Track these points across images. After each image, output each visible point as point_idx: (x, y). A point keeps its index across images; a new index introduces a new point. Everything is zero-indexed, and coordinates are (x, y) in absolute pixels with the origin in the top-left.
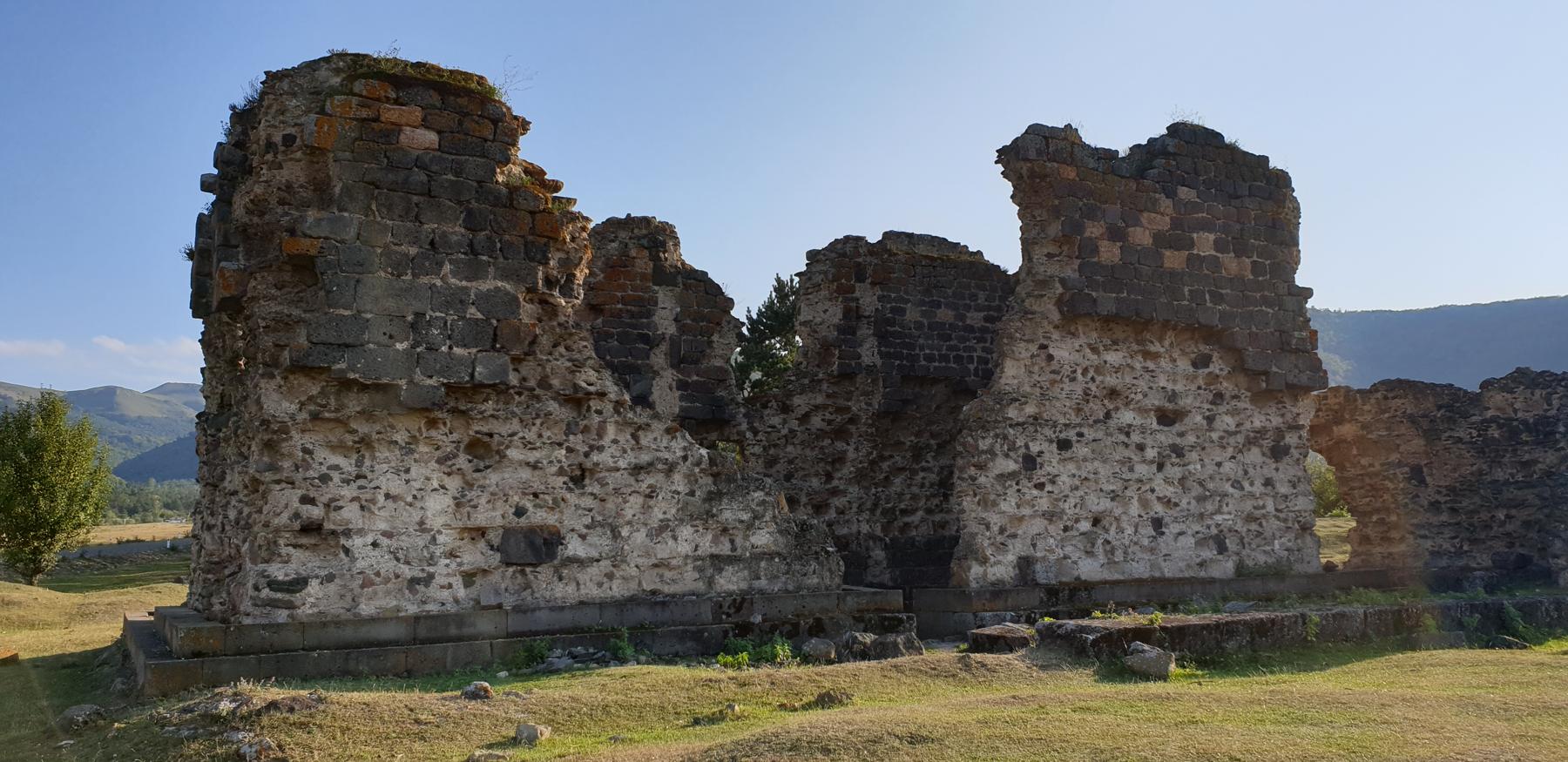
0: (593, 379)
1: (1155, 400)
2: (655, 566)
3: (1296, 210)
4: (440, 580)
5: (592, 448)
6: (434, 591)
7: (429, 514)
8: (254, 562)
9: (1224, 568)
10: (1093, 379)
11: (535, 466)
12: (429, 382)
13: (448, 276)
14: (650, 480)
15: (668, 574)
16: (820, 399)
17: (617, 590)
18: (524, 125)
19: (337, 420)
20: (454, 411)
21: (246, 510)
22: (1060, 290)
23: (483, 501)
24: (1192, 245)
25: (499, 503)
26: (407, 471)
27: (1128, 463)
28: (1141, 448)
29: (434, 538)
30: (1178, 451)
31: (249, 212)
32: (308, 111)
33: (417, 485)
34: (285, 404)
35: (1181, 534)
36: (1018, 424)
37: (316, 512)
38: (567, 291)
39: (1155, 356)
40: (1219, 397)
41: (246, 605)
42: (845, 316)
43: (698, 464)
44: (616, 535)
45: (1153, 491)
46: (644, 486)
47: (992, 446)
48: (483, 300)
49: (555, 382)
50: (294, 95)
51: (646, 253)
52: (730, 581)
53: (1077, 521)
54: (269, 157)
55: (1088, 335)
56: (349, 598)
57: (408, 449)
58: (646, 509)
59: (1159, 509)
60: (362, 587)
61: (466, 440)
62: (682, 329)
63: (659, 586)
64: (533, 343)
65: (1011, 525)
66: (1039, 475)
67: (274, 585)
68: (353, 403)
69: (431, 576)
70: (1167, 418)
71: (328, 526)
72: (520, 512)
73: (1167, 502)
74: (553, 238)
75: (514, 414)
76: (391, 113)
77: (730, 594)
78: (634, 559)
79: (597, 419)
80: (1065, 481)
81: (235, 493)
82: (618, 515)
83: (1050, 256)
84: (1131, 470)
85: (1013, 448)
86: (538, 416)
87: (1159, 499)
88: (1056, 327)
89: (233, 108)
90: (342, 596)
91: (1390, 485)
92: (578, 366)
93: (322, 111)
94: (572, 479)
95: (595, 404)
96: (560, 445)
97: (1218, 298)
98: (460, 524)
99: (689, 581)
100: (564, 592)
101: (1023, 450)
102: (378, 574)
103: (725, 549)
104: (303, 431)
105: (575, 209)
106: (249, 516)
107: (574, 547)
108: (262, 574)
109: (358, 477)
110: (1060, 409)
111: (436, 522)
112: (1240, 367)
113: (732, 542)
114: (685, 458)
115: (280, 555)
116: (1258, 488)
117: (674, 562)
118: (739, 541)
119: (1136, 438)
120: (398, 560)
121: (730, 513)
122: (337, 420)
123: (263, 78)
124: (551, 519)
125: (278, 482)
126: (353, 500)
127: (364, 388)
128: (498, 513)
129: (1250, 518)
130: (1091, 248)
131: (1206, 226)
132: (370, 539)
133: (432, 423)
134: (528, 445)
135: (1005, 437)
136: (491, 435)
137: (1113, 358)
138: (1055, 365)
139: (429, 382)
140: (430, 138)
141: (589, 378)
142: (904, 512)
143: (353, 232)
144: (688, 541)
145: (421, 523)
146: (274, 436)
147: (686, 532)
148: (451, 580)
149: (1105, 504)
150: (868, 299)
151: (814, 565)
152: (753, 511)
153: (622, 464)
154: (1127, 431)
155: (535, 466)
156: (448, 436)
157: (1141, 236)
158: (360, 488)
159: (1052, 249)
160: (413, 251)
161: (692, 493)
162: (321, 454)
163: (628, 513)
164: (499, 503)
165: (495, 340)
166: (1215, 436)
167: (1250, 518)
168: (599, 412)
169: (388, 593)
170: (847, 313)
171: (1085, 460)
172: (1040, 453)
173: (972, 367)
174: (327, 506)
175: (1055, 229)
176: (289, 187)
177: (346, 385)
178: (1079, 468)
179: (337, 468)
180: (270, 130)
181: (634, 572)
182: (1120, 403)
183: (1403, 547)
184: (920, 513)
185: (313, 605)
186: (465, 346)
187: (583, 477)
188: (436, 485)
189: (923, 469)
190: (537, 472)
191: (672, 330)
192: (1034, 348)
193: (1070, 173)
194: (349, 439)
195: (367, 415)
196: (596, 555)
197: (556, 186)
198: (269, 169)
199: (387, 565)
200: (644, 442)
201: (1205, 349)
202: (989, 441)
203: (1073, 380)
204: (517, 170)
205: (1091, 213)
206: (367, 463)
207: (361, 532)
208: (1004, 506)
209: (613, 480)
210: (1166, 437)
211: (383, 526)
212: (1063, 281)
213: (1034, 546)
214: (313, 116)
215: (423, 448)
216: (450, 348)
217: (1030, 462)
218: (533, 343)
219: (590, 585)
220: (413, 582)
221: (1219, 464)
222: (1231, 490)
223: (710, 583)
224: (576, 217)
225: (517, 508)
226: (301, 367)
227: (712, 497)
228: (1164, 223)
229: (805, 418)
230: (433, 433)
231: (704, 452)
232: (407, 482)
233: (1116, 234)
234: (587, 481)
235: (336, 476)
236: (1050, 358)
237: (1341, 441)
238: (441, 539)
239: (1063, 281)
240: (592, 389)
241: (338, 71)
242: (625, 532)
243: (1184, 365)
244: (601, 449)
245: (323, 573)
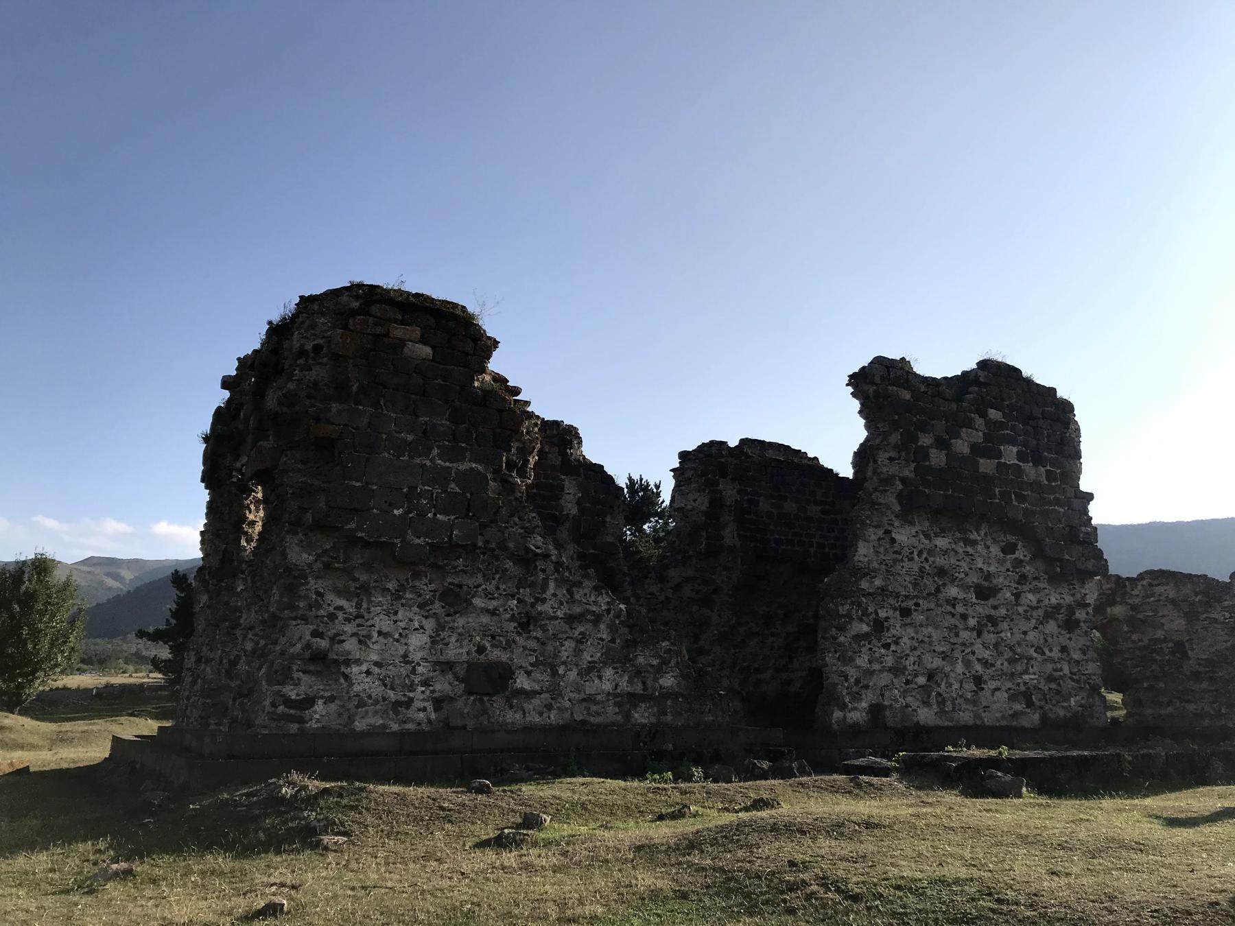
0: (540, 544)
1: (974, 579)
2: (584, 700)
3: (1078, 430)
4: (418, 704)
5: (537, 600)
6: (411, 713)
7: (411, 649)
8: (269, 683)
9: (1033, 719)
10: (926, 560)
11: (493, 613)
12: (418, 541)
13: (435, 458)
14: (581, 629)
15: (594, 708)
16: (690, 572)
17: (554, 718)
18: (495, 344)
19: (344, 570)
20: (434, 566)
21: (262, 643)
22: (900, 487)
23: (453, 639)
24: (999, 455)
25: (465, 642)
26: (396, 613)
27: (954, 629)
28: (964, 617)
29: (414, 669)
30: (993, 621)
31: (280, 403)
32: (334, 327)
33: (402, 624)
34: (305, 556)
35: (998, 689)
36: (869, 594)
37: (324, 644)
38: (523, 475)
39: (973, 543)
40: (1023, 579)
41: (261, 719)
42: (710, 503)
43: (618, 616)
44: (554, 673)
45: (973, 653)
46: (577, 633)
47: (850, 611)
48: (463, 478)
49: (511, 545)
50: (323, 314)
51: (556, 449)
52: (642, 716)
53: (916, 676)
54: (301, 361)
56: (345, 716)
57: (397, 596)
58: (578, 652)
59: (979, 667)
60: (357, 707)
61: (441, 590)
62: (582, 510)
63: (587, 718)
64: (496, 512)
65: (869, 675)
66: (887, 637)
67: (288, 702)
68: (358, 558)
69: (411, 700)
70: (984, 593)
71: (333, 656)
72: (481, 650)
73: (985, 663)
74: (516, 431)
75: (479, 570)
76: (398, 332)
77: (643, 726)
78: (569, 694)
79: (542, 576)
81: (252, 628)
82: (556, 656)
83: (891, 459)
84: (957, 635)
85: (865, 613)
86: (497, 572)
87: (978, 660)
88: (897, 516)
89: (270, 323)
90: (340, 715)
91: (1158, 658)
92: (529, 532)
93: (345, 327)
94: (520, 625)
95: (540, 564)
96: (513, 596)
97: (1021, 498)
98: (434, 659)
99: (611, 713)
100: (513, 717)
102: (370, 697)
103: (638, 688)
104: (317, 578)
105: (529, 409)
106: (266, 645)
107: (522, 682)
108: (278, 693)
109: (357, 617)
110: (902, 583)
111: (417, 656)
112: (1039, 554)
113: (644, 683)
114: (608, 611)
115: (292, 679)
116: (1056, 654)
117: (599, 697)
118: (649, 682)
119: (960, 609)
120: (385, 685)
121: (643, 659)
122: (344, 570)
123: (297, 300)
124: (504, 657)
125: (295, 619)
126: (353, 635)
127: (367, 544)
128: (464, 650)
129: (1050, 679)
130: (923, 453)
131: (1011, 441)
132: (364, 668)
133: (417, 575)
134: (489, 596)
135: (859, 605)
136: (460, 586)
137: (941, 543)
138: (896, 547)
139: (418, 541)
140: (427, 351)
141: (536, 542)
142: (757, 670)
143: (366, 421)
144: (608, 681)
145: (405, 656)
146: (293, 579)
147: (608, 673)
148: (426, 704)
149: (938, 662)
150: (729, 492)
151: (709, 706)
152: (661, 657)
153: (559, 614)
154: (953, 602)
155: (493, 613)
156: (426, 587)
157: (961, 446)
158: (359, 625)
159: (893, 454)
160: (410, 438)
162: (330, 597)
163: (564, 655)
164: (465, 642)
165: (468, 510)
166: (1021, 609)
167: (1050, 679)
168: (543, 571)
169: (376, 713)
170: (713, 503)
171: (921, 626)
172: (887, 619)
173: (812, 550)
174: (332, 639)
175: (895, 438)
176: (316, 384)
177: (353, 541)
178: (917, 633)
179: (341, 608)
180: (303, 341)
181: (567, 704)
182: (946, 580)
183: (1170, 709)
184: (770, 672)
185: (318, 721)
186: (446, 514)
187: (528, 624)
188: (417, 625)
189: (773, 635)
190: (495, 618)
191: (574, 511)
192: (880, 533)
193: (906, 395)
194: (352, 585)
195: (367, 567)
196: (537, 688)
197: (516, 391)
198: (301, 371)
199: (377, 690)
200: (577, 597)
201: (1012, 539)
202: (847, 607)
203: (911, 559)
204: (488, 378)
205: (923, 427)
206: (365, 605)
207: (358, 662)
208: (859, 662)
209: (552, 626)
210: (983, 609)
211: (375, 657)
212: (903, 480)
213: (882, 695)
214: (339, 331)
215: (408, 595)
216: (435, 515)
217: (879, 626)
218: (496, 512)
219: (533, 714)
220: (398, 704)
221: (1025, 633)
222: (1035, 655)
223: (628, 716)
224: (531, 415)
225: (479, 646)
226: (321, 526)
227: (630, 644)
228: (978, 437)
229: (678, 588)
230: (417, 583)
231: (622, 606)
232: (395, 622)
233: (942, 444)
234: (532, 627)
235: (340, 615)
236: (893, 541)
237: (1114, 619)
238: (420, 669)
239: (903, 480)
240: (539, 551)
241: (357, 297)
242: (561, 671)
243: (995, 550)
244: (544, 601)
245: (327, 694)
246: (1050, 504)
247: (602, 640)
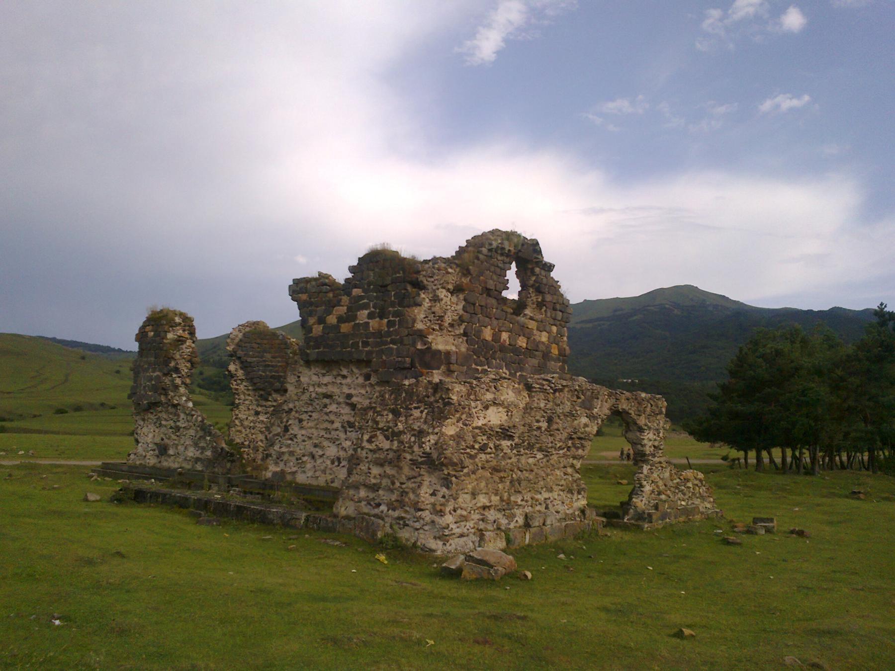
39: (344, 377)
53: (304, 456)
72: (162, 439)
97: (366, 344)
131: (365, 307)
137: (326, 380)
157: (332, 319)
217: (286, 429)
243: (361, 380)
246: (386, 343)
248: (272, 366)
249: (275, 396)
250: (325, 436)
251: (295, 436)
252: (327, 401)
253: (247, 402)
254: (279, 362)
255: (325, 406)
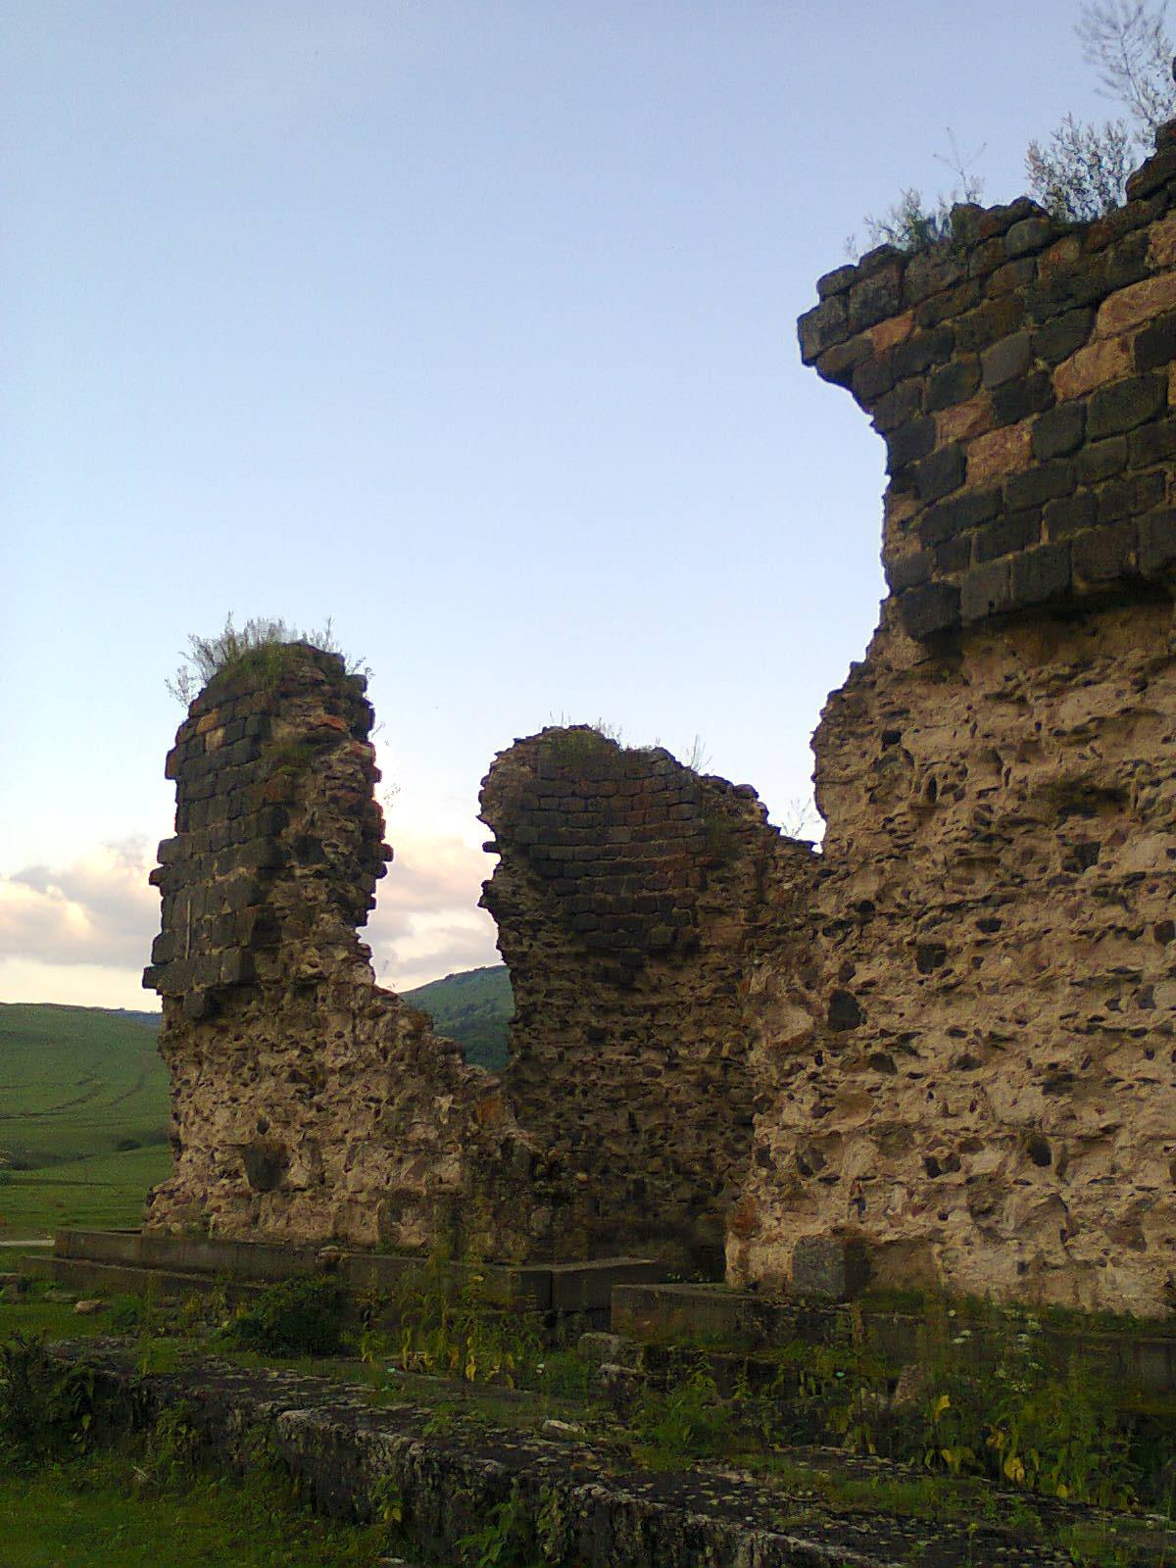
36: (840, 924)
53: (971, 1146)
55: (995, 668)
66: (861, 1039)
72: (263, 1128)
80: (936, 1048)
84: (1146, 1002)
101: (833, 984)
137: (1074, 709)
149: (1034, 1103)
161: (390, 1102)
182: (1123, 821)
192: (875, 748)
213: (860, 1202)
217: (845, 1012)
244: (321, 1046)
247: (378, 1101)
248: (639, 868)
249: (655, 971)
250: (1115, 1020)
251: (905, 1043)
252: (1095, 829)
253: (556, 1001)
254: (661, 850)
255: (1084, 854)
